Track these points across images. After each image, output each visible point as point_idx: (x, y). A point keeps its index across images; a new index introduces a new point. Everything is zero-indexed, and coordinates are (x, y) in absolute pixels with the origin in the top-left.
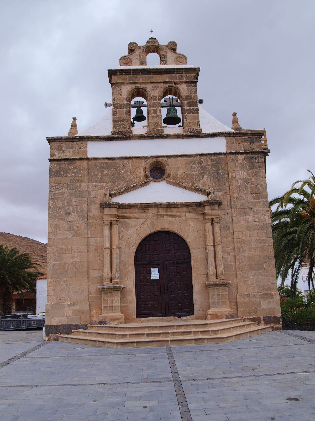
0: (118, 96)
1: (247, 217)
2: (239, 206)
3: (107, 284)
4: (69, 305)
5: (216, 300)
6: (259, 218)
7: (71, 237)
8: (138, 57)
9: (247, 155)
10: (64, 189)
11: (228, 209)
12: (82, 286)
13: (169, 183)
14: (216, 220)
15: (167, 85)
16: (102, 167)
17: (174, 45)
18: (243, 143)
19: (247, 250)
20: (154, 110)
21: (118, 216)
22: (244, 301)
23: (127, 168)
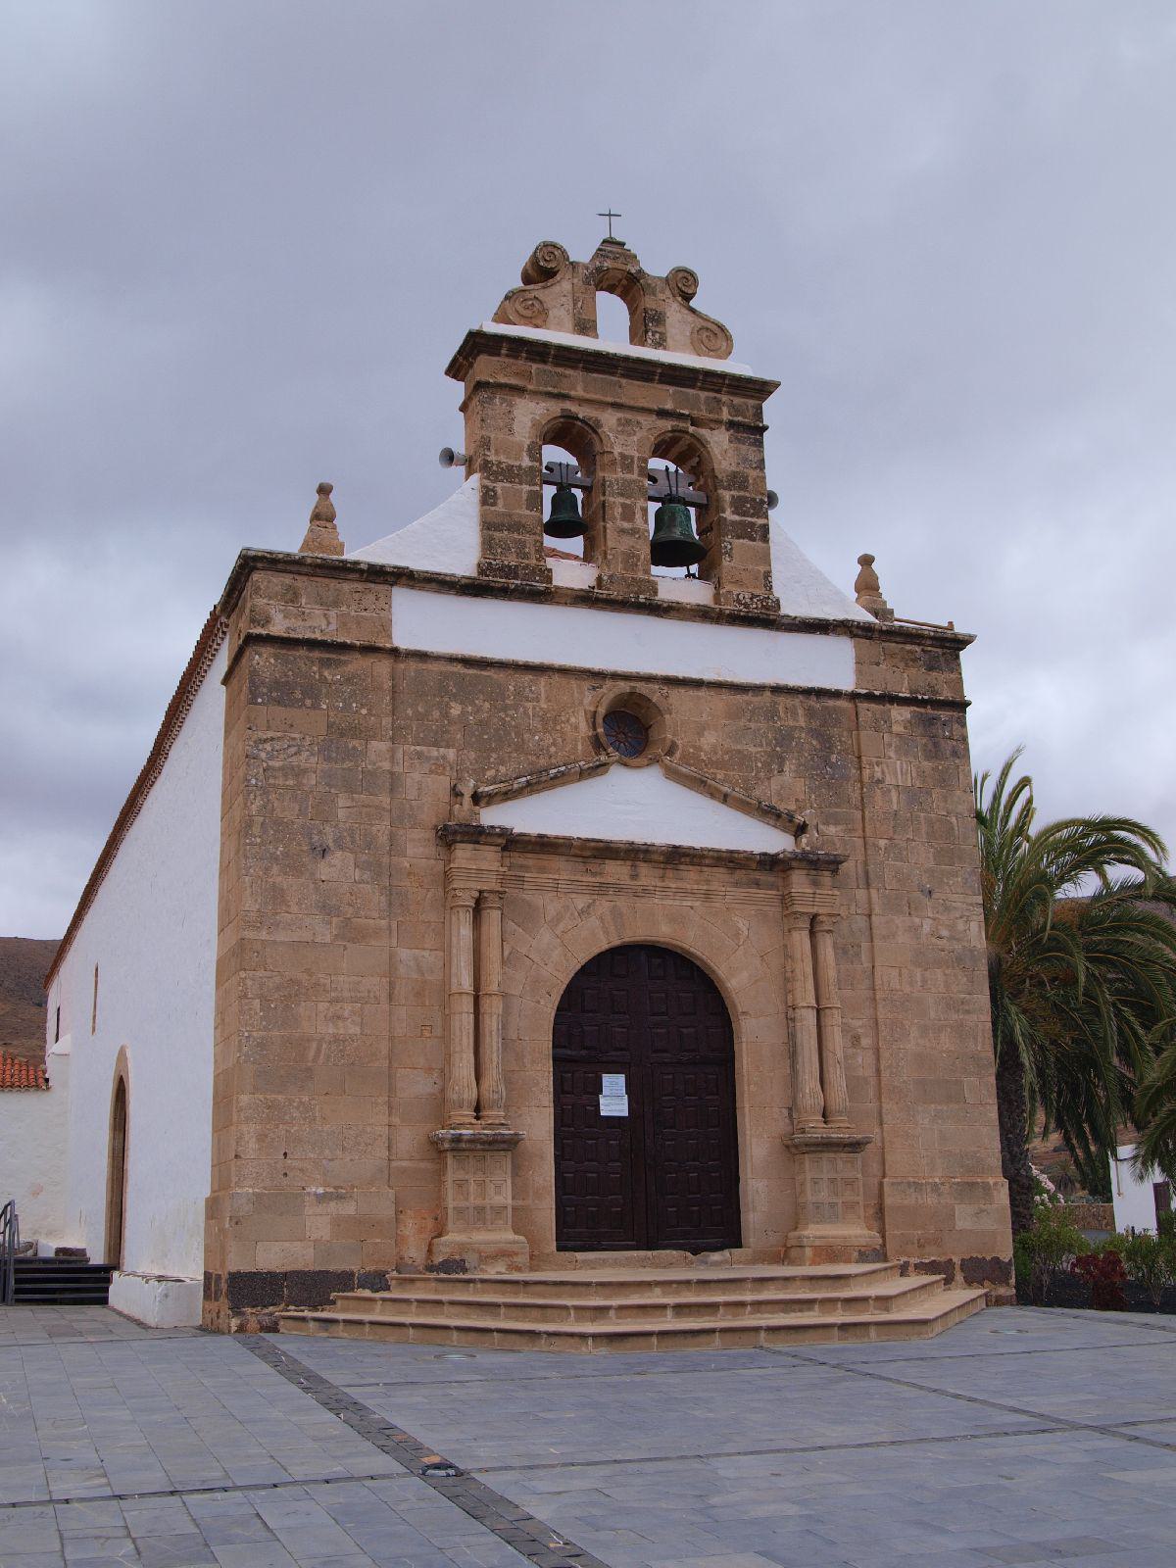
0: (501, 436)
1: (917, 920)
4: (321, 1199)
6: (952, 927)
7: (328, 939)
8: (568, 302)
9: (918, 709)
10: (305, 754)
11: (858, 887)
12: (369, 1129)
13: (673, 775)
15: (668, 425)
17: (690, 283)
18: (907, 665)
19: (914, 1032)
20: (623, 506)
21: (503, 879)
22: (906, 1202)
23: (529, 705)
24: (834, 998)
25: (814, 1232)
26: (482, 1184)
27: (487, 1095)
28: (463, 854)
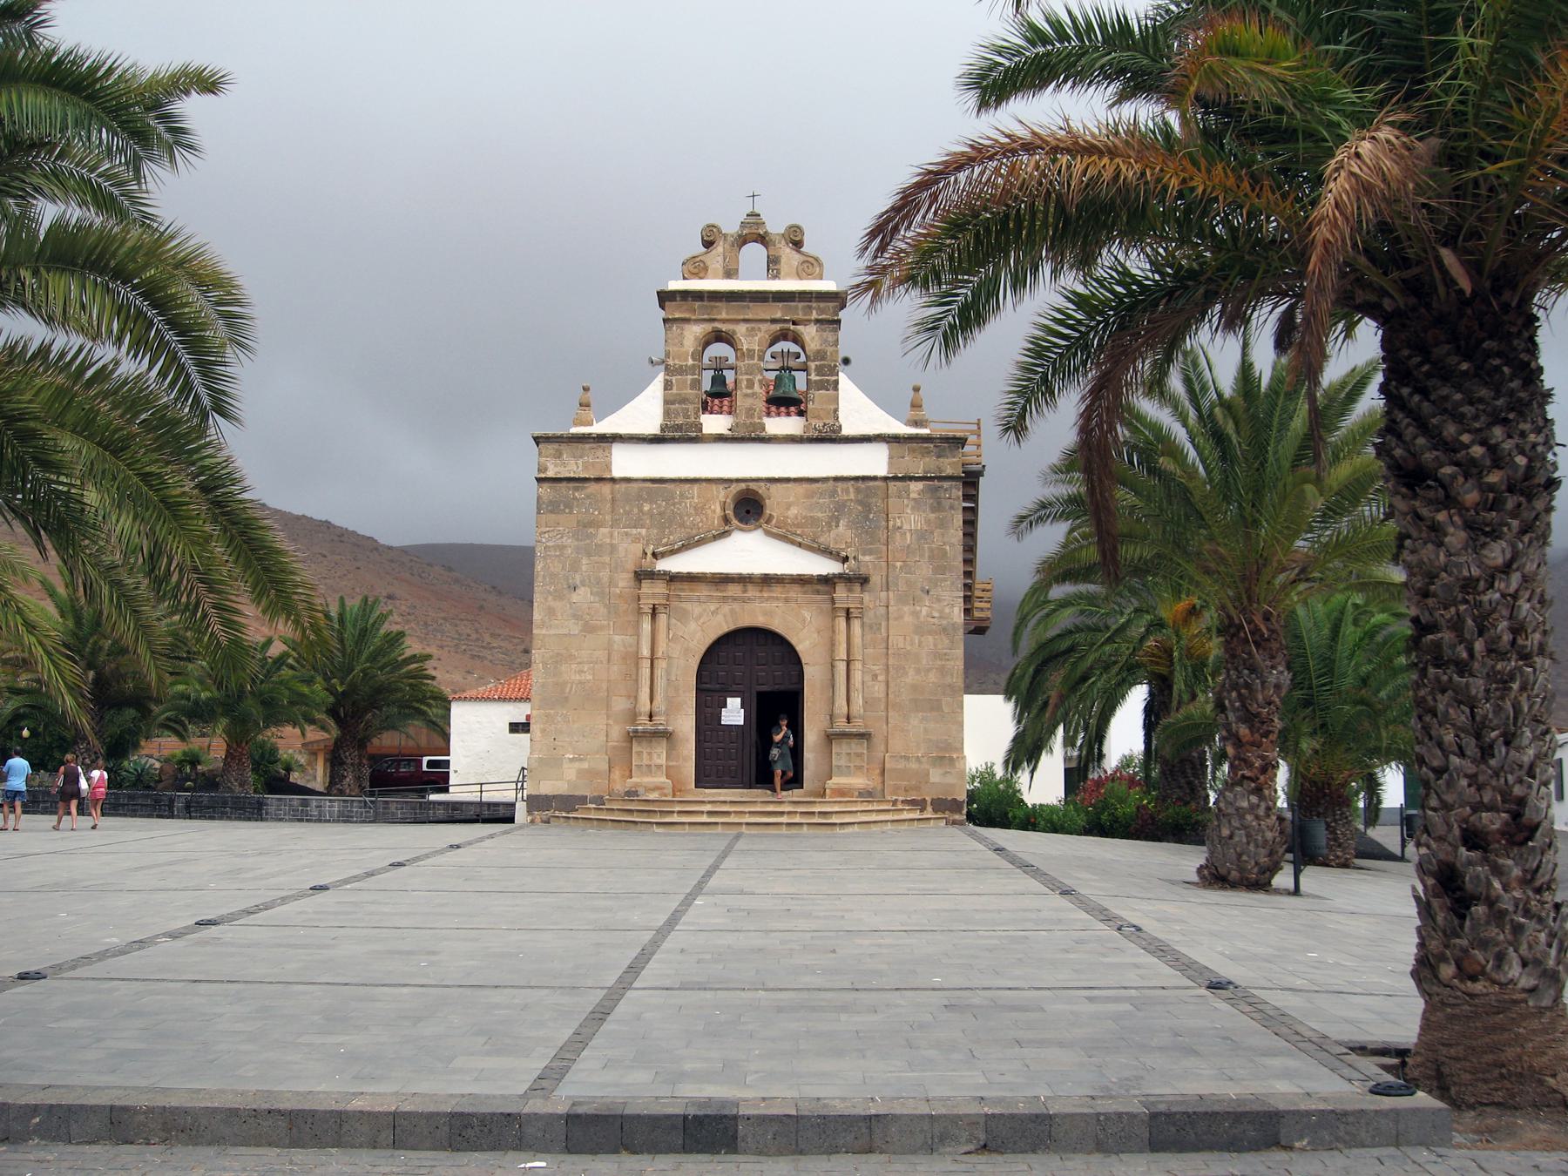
2: (902, 587)
3: (643, 724)
4: (572, 760)
5: (843, 762)
6: (941, 612)
8: (720, 259)
13: (768, 533)
14: (854, 613)
15: (778, 327)
16: (639, 497)
19: (911, 672)
21: (668, 597)
24: (857, 654)
25: (837, 781)
26: (650, 754)
27: (655, 709)
28: (647, 587)
